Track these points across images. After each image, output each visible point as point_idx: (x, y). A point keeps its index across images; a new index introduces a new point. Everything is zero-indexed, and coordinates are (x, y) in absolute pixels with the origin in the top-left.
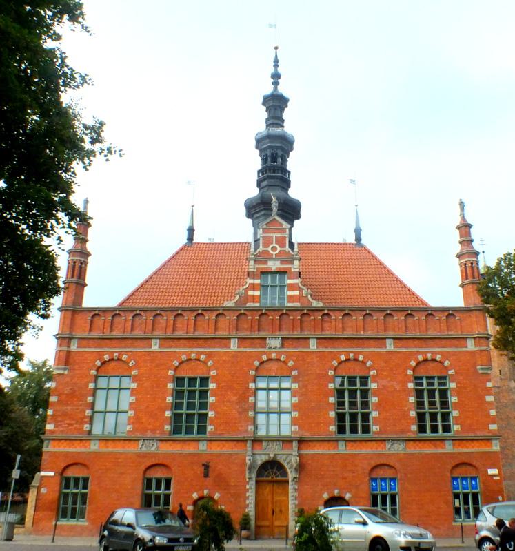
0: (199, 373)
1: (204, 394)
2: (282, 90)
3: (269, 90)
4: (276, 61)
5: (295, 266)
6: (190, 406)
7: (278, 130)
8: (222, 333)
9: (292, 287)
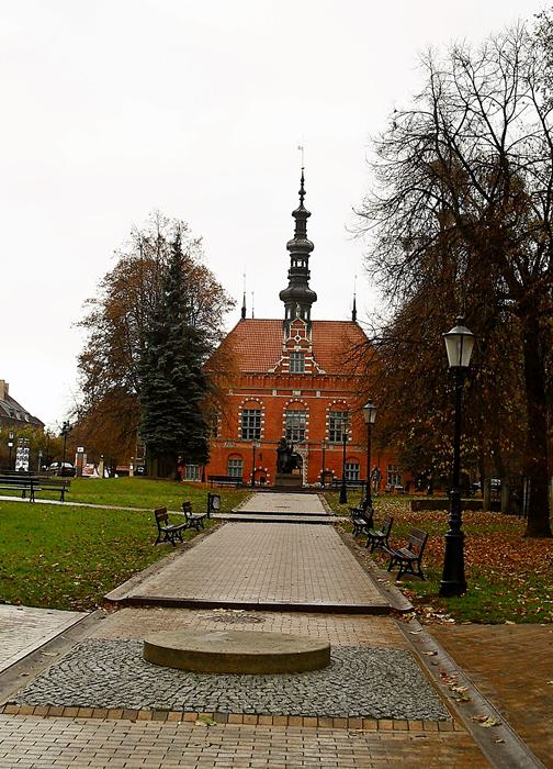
0: (256, 408)
1: (258, 419)
2: (308, 207)
3: (296, 206)
4: (303, 180)
5: (310, 350)
6: (251, 424)
7: (302, 242)
8: (267, 387)
9: (308, 362)
